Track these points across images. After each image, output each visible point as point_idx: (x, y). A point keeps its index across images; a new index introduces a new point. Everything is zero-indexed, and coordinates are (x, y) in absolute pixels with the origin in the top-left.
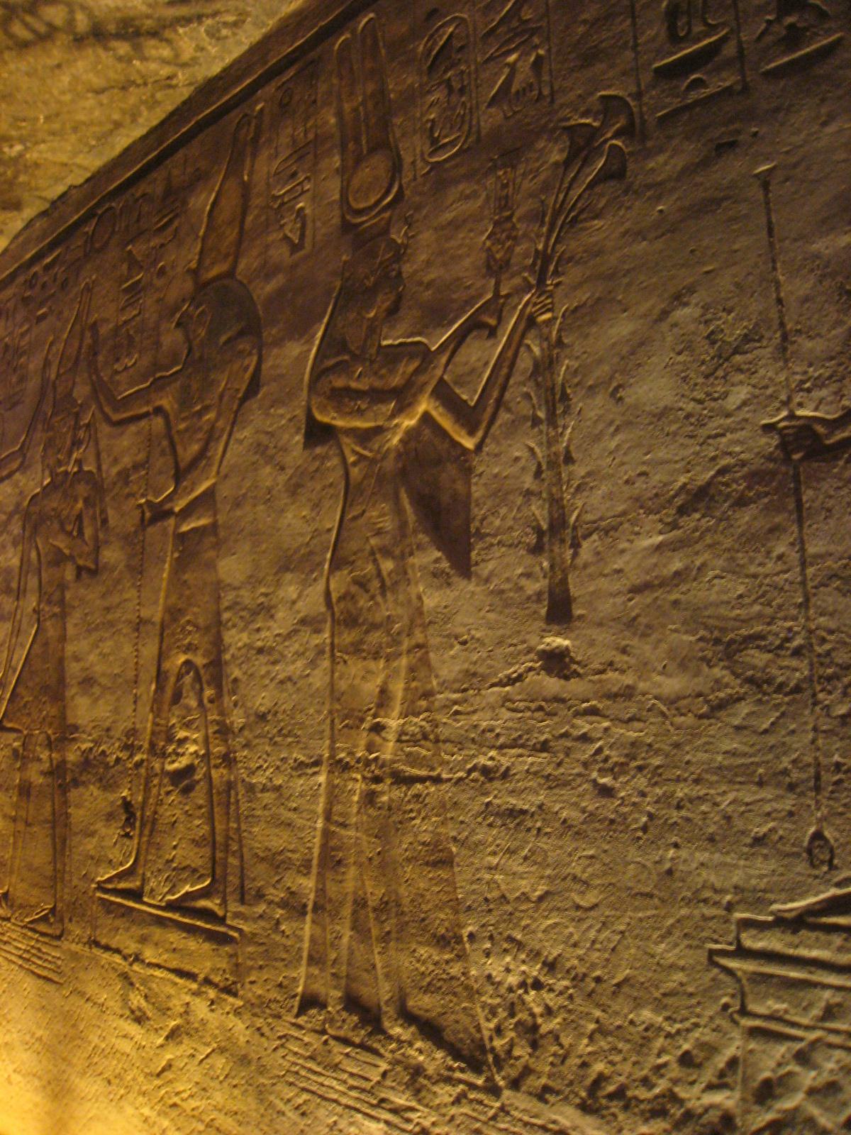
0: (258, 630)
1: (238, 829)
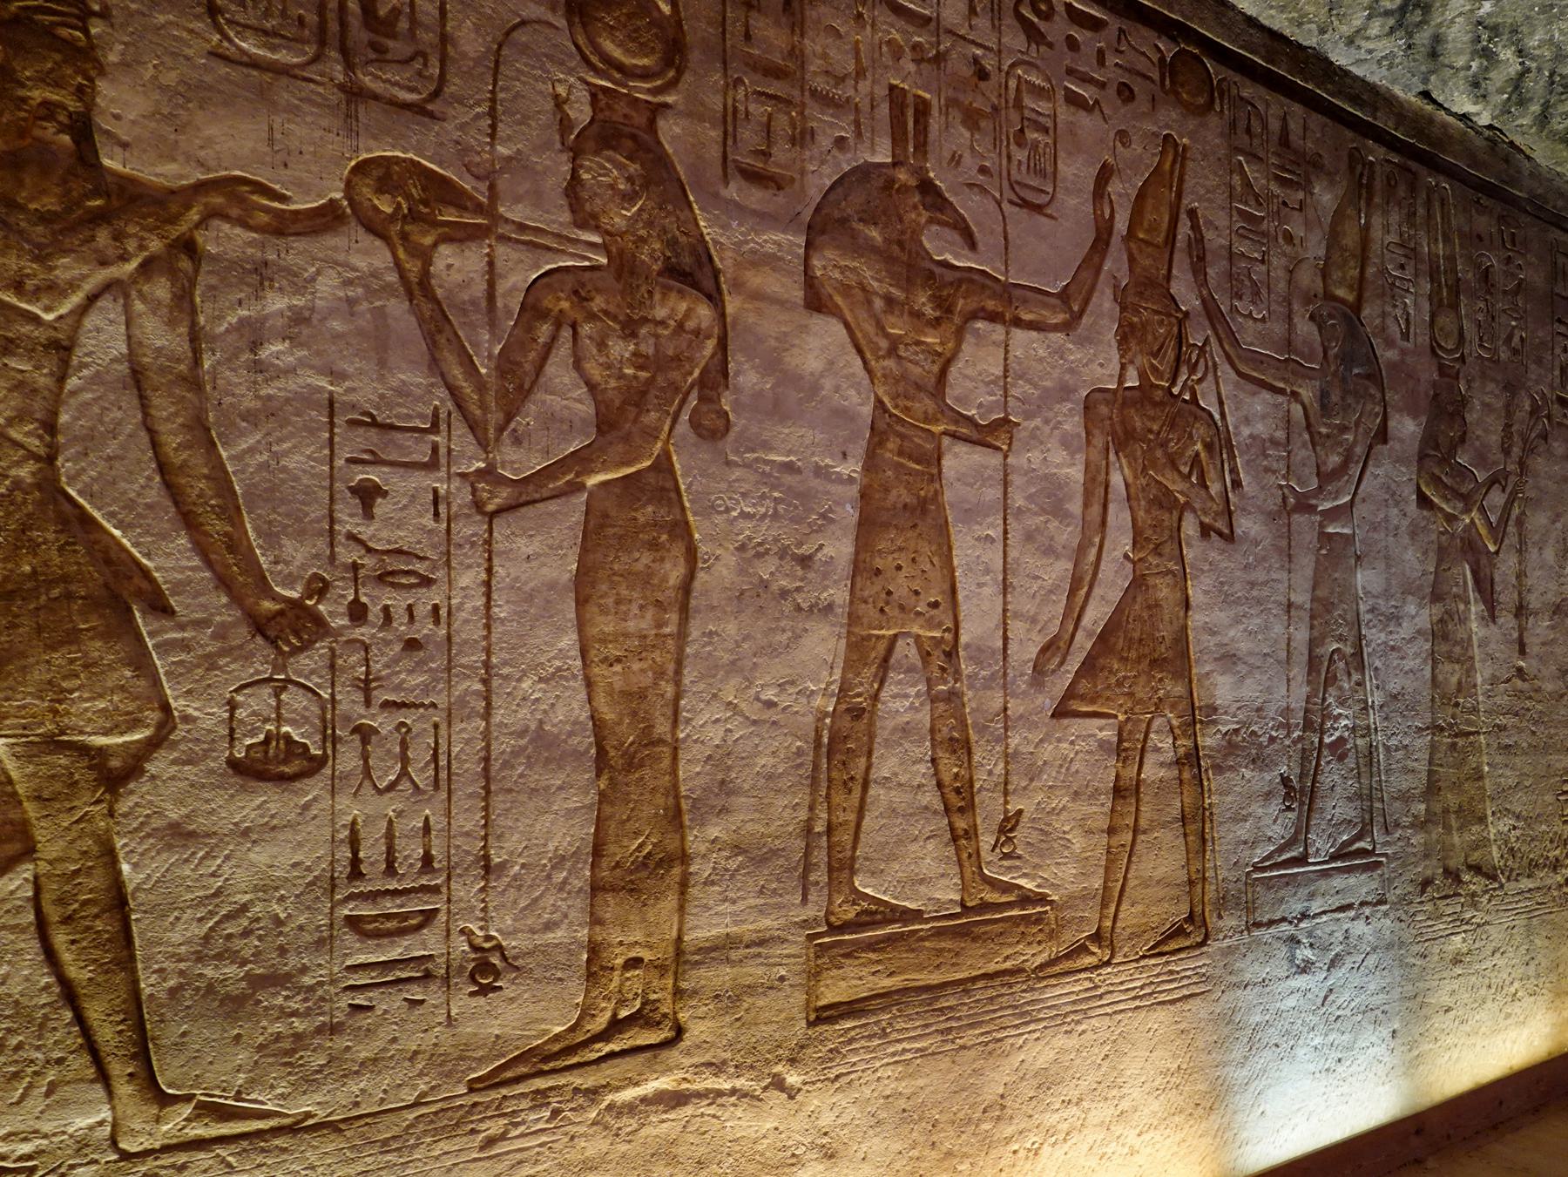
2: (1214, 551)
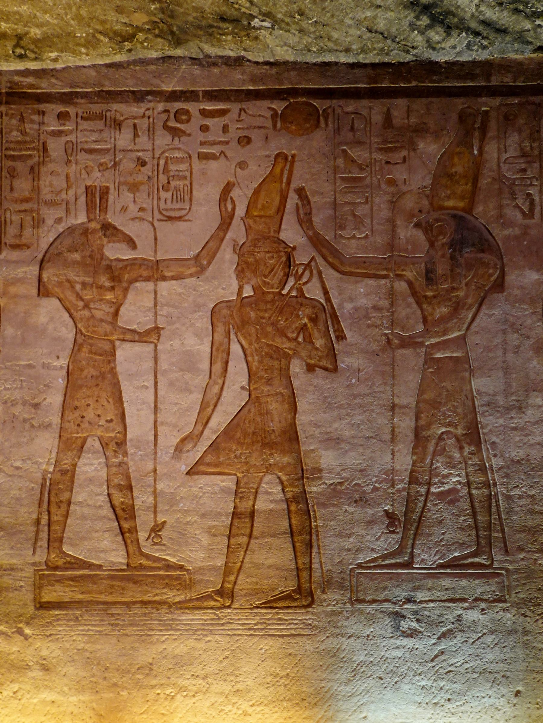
0: (512, 418)
1: (500, 518)
2: (319, 378)
